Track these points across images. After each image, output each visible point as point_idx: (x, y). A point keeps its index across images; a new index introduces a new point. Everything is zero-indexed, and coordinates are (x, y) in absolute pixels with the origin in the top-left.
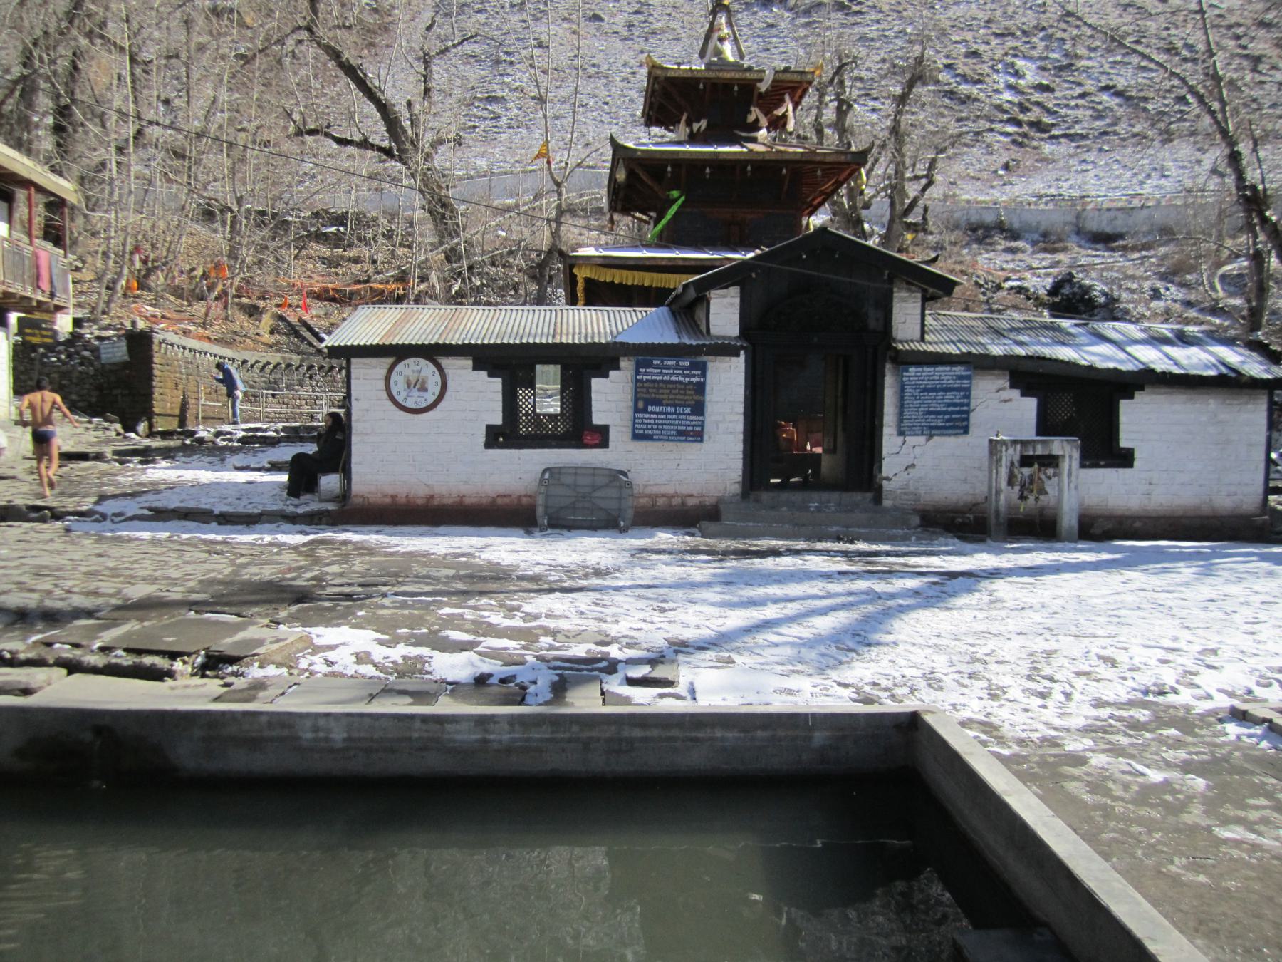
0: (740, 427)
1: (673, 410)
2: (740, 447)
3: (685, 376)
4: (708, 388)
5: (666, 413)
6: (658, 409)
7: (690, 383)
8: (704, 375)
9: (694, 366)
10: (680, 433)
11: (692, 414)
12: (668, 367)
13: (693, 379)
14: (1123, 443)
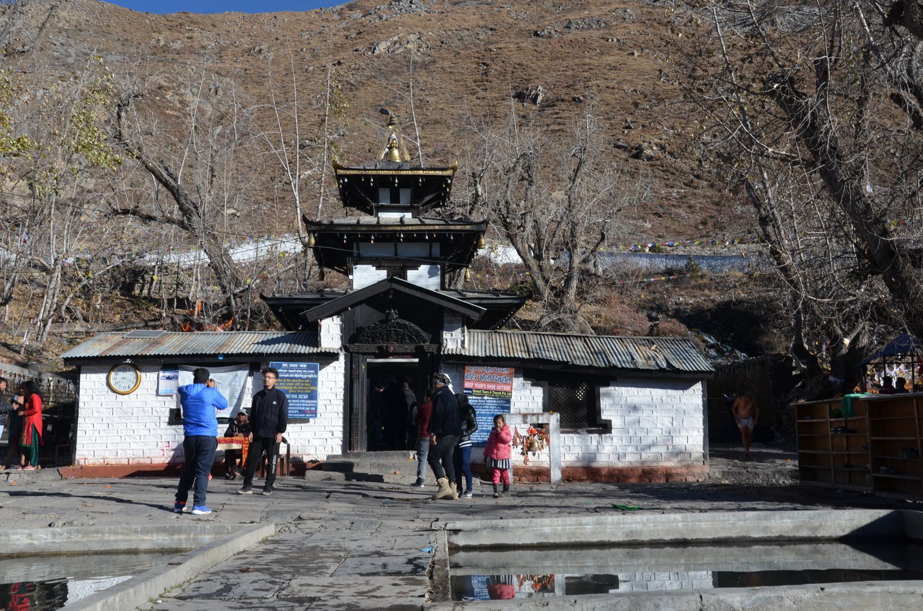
0: (341, 409)
3: (303, 374)
7: (307, 378)
8: (316, 373)
9: (308, 368)
12: (292, 368)
14: (605, 416)
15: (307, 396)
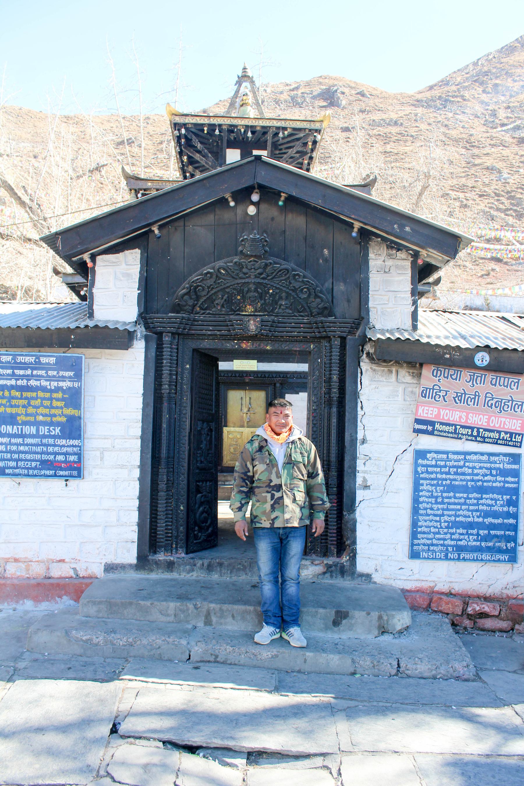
1: (33, 430)
2: (134, 489)
3: (50, 379)
4: (86, 400)
5: (23, 436)
6: (9, 429)
7: (58, 389)
8: (78, 376)
9: (61, 364)
10: (46, 464)
11: (64, 435)
12: (24, 366)
13: (61, 384)
15: (58, 431)
